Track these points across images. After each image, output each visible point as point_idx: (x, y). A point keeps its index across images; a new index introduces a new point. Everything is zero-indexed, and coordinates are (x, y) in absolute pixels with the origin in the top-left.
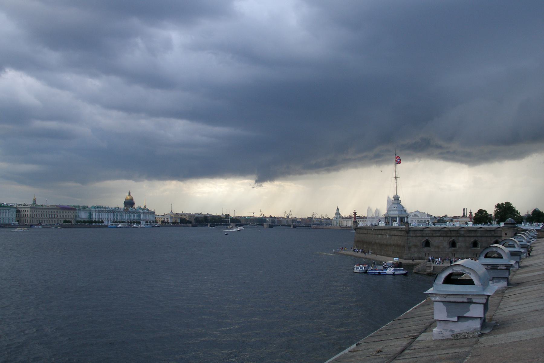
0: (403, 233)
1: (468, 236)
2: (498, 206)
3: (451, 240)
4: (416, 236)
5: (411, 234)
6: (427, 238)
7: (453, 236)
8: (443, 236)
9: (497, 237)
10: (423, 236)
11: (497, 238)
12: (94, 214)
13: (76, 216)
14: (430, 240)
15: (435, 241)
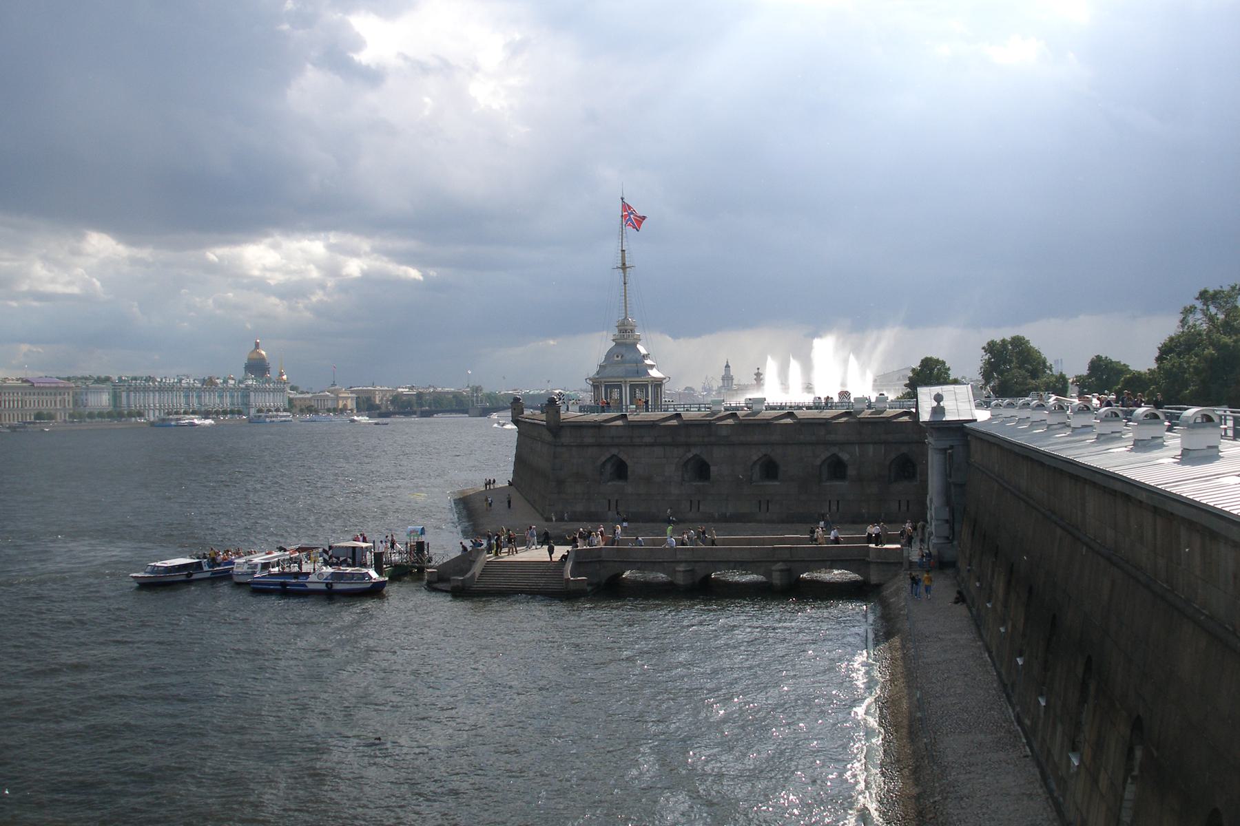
0: (547, 436)
1: (742, 444)
2: (991, 348)
3: (690, 455)
4: (581, 446)
5: (566, 438)
6: (614, 451)
7: (695, 445)
8: (663, 445)
9: (834, 444)
10: (600, 445)
11: (835, 450)
12: (124, 394)
13: (76, 403)
14: (623, 457)
15: (639, 461)
